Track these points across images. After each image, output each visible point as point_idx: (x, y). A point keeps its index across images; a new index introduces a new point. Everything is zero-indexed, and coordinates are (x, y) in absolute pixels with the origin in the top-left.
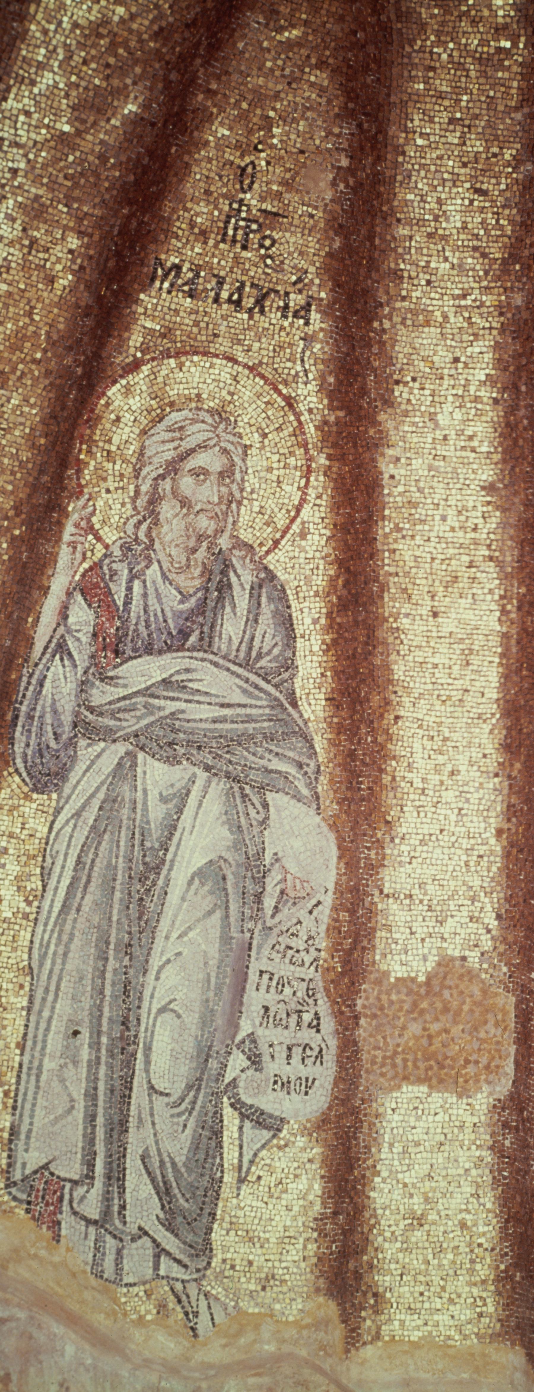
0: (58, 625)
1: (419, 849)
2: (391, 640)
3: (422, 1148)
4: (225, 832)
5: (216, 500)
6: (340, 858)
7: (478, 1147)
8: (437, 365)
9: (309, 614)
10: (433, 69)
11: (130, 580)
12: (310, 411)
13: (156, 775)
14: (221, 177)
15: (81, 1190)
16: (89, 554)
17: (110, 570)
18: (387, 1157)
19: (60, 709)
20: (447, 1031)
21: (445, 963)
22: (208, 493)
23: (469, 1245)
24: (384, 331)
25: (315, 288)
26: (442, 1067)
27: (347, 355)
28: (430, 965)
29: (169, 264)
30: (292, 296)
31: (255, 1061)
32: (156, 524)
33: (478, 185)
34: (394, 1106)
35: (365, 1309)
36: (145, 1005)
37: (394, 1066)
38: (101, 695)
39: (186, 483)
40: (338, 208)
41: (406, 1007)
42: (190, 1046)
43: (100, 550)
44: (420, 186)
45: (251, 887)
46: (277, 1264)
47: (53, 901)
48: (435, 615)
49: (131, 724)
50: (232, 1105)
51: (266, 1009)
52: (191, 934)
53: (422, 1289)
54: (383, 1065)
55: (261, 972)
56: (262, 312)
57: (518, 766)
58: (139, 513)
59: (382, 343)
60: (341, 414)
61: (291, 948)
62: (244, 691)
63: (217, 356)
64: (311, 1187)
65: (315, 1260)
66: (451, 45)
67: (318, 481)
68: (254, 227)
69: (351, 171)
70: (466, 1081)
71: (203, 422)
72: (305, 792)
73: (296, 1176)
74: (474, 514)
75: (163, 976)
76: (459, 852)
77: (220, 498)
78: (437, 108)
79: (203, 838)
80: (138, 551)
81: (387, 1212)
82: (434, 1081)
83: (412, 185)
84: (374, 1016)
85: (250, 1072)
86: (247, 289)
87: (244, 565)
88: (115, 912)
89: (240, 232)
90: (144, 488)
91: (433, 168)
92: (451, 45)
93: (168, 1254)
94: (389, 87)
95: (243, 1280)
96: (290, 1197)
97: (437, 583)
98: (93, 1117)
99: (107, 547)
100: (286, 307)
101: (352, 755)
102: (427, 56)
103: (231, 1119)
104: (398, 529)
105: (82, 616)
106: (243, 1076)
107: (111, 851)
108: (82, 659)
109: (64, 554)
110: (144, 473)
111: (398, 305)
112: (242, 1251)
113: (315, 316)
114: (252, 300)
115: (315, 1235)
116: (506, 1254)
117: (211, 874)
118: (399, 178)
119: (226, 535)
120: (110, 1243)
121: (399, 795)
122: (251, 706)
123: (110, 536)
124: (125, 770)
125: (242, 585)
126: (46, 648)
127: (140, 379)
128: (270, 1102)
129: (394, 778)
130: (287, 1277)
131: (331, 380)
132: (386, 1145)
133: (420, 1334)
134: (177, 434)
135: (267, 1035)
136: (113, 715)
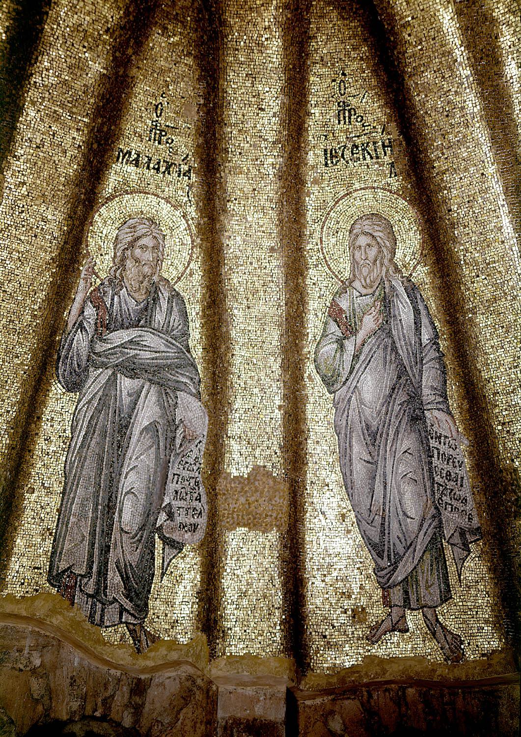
0: (79, 316)
1: (244, 415)
2: (229, 320)
3: (246, 558)
4: (157, 409)
5: (151, 259)
6: (209, 421)
7: (272, 557)
8: (246, 192)
9: (194, 310)
10: (237, 50)
12: (192, 219)
13: (126, 384)
14: (147, 110)
15: (86, 580)
16: (93, 284)
18: (230, 564)
20: (257, 501)
21: (256, 468)
22: (148, 256)
23: (268, 606)
24: (221, 177)
25: (192, 162)
26: (255, 518)
27: (208, 191)
28: (249, 470)
29: (125, 151)
30: (182, 166)
31: (171, 516)
33: (260, 106)
34: (233, 537)
35: (219, 639)
36: (120, 490)
37: (233, 518)
38: (99, 347)
39: (138, 252)
40: (200, 124)
41: (238, 490)
42: (140, 509)
43: (98, 282)
44: (234, 107)
45: (170, 435)
46: (179, 615)
47: (76, 442)
48: (249, 308)
49: (114, 360)
50: (159, 537)
51: (176, 492)
52: (142, 457)
53: (246, 628)
54: (228, 518)
55: (174, 475)
56: (169, 173)
57: (288, 376)
59: (221, 183)
60: (206, 219)
61: (188, 463)
62: (166, 345)
63: (149, 194)
64: (195, 577)
65: (197, 613)
66: (245, 37)
67: (197, 251)
68: (163, 133)
69: (205, 105)
70: (266, 525)
72: (194, 391)
73: (189, 571)
74: (265, 261)
75: (128, 477)
76: (261, 416)
78: (240, 69)
79: (147, 412)
80: (116, 282)
81: (229, 590)
82: (252, 525)
83: (231, 107)
84: (224, 494)
85: (168, 522)
86: (162, 163)
87: (165, 289)
88: (106, 447)
89: (157, 136)
90: (118, 254)
91: (240, 99)
92: (245, 37)
93: (128, 611)
94: (218, 61)
95: (163, 623)
96: (186, 582)
97: (249, 293)
98: (93, 544)
100: (180, 171)
101: (214, 373)
102: (234, 43)
103: (159, 544)
104: (231, 269)
105: (90, 311)
106: (165, 524)
107: (104, 418)
108: (91, 330)
109: (82, 283)
110: (118, 246)
111: (227, 165)
112: (162, 609)
113: (193, 175)
114: (164, 168)
115: (197, 600)
116: (286, 610)
117: (152, 428)
118: (225, 104)
119: (156, 275)
120: (99, 605)
121: (234, 391)
122: (169, 352)
123: (103, 275)
124: (112, 382)
125: (164, 298)
127: (114, 203)
128: (176, 536)
129: (232, 383)
130: (184, 622)
131: (201, 204)
132: (229, 557)
133: (244, 652)
134: (133, 230)
135: (176, 504)
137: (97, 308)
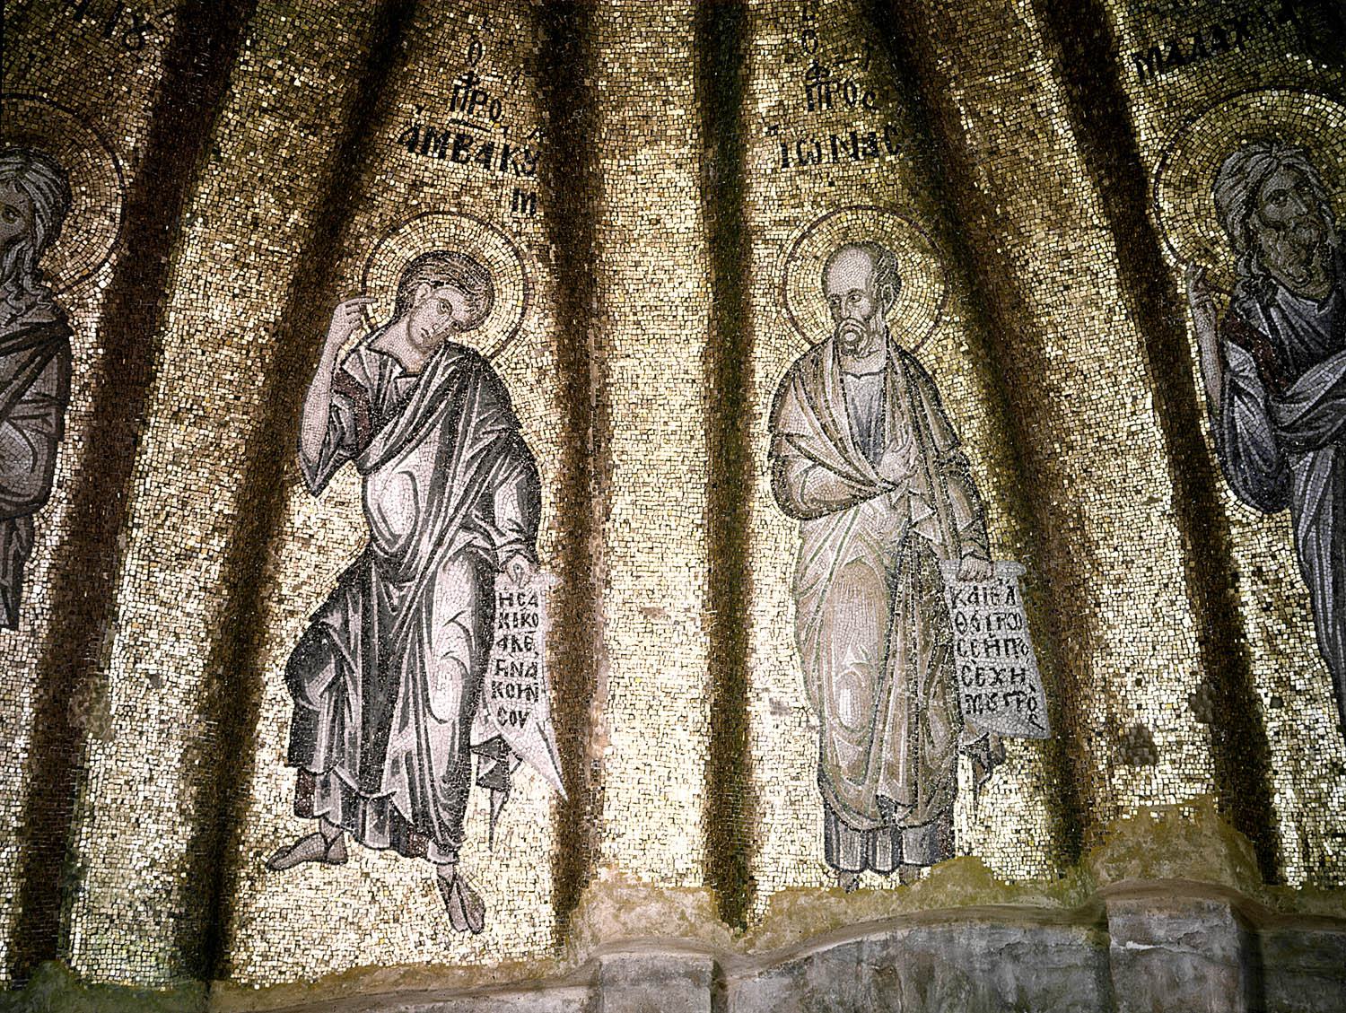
0: (1223, 373)
11: (1265, 309)
16: (1219, 306)
17: (1244, 310)
19: (1260, 439)
32: (1263, 256)
38: (1289, 414)
58: (1243, 255)
71: (1256, 153)
77: (1308, 206)
90: (1236, 233)
99: (1229, 293)
105: (1238, 357)
110: (1229, 219)
119: (1331, 235)
126: (1223, 393)
136: (1308, 425)
137: (1246, 346)
